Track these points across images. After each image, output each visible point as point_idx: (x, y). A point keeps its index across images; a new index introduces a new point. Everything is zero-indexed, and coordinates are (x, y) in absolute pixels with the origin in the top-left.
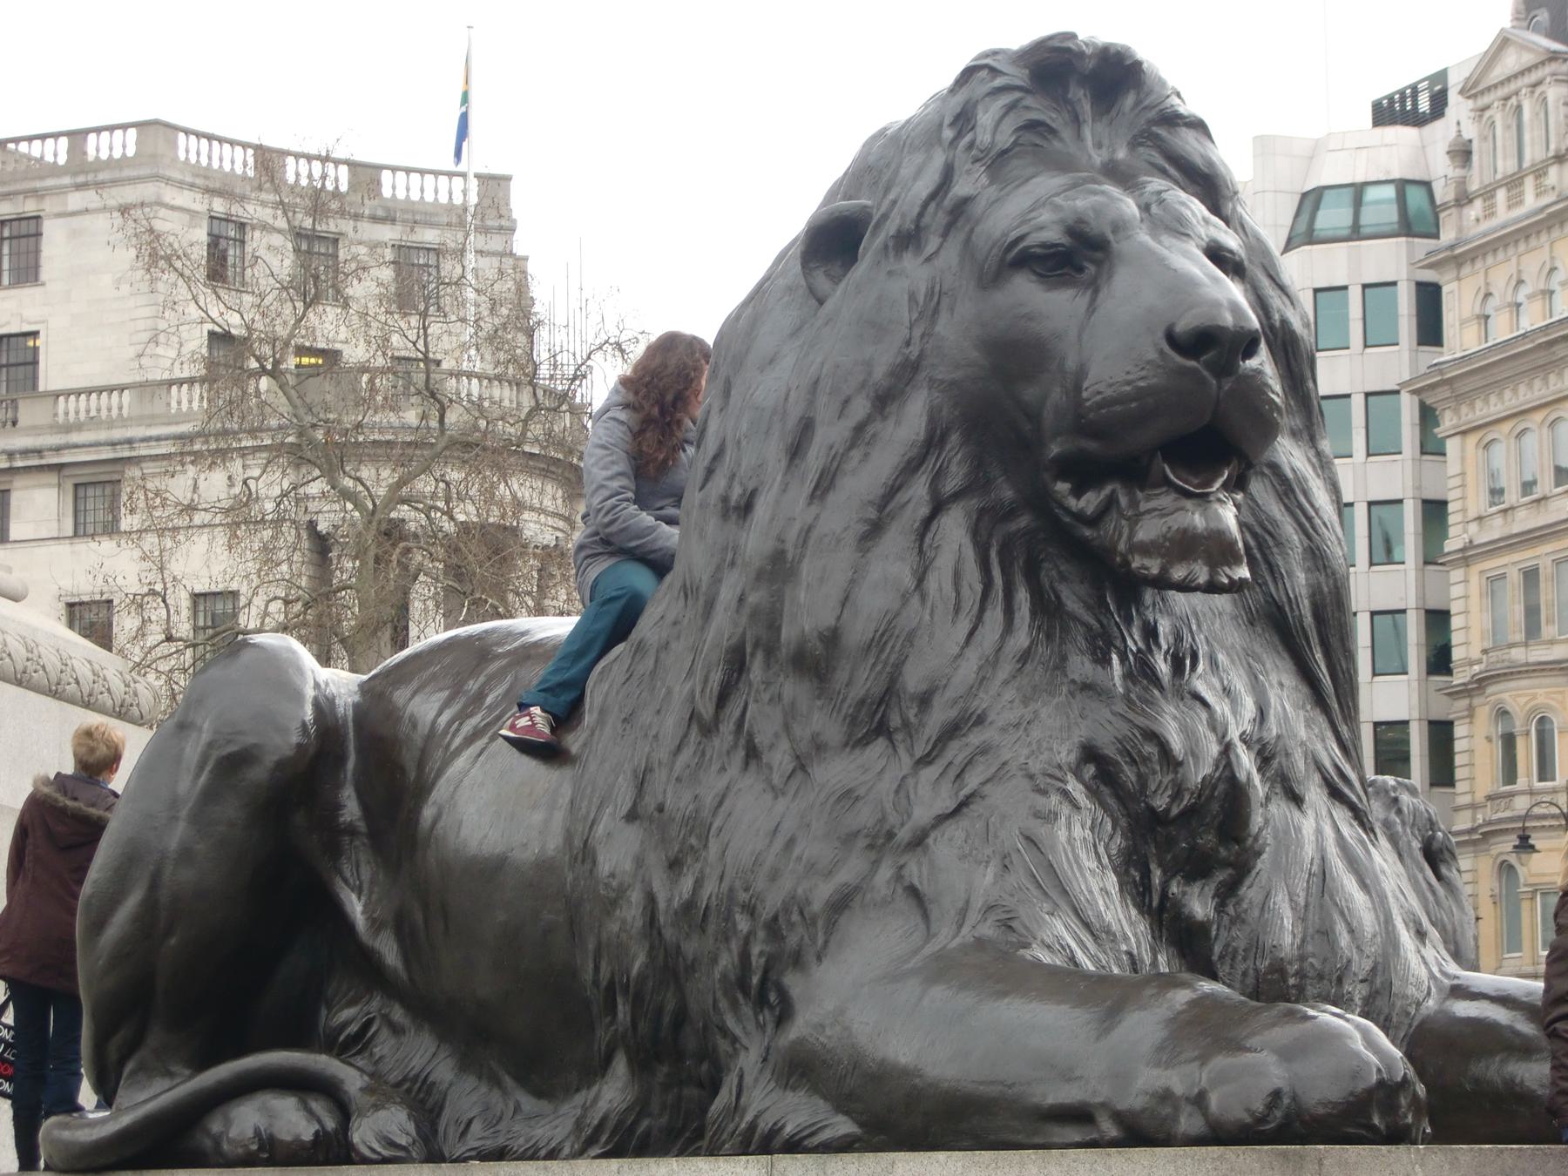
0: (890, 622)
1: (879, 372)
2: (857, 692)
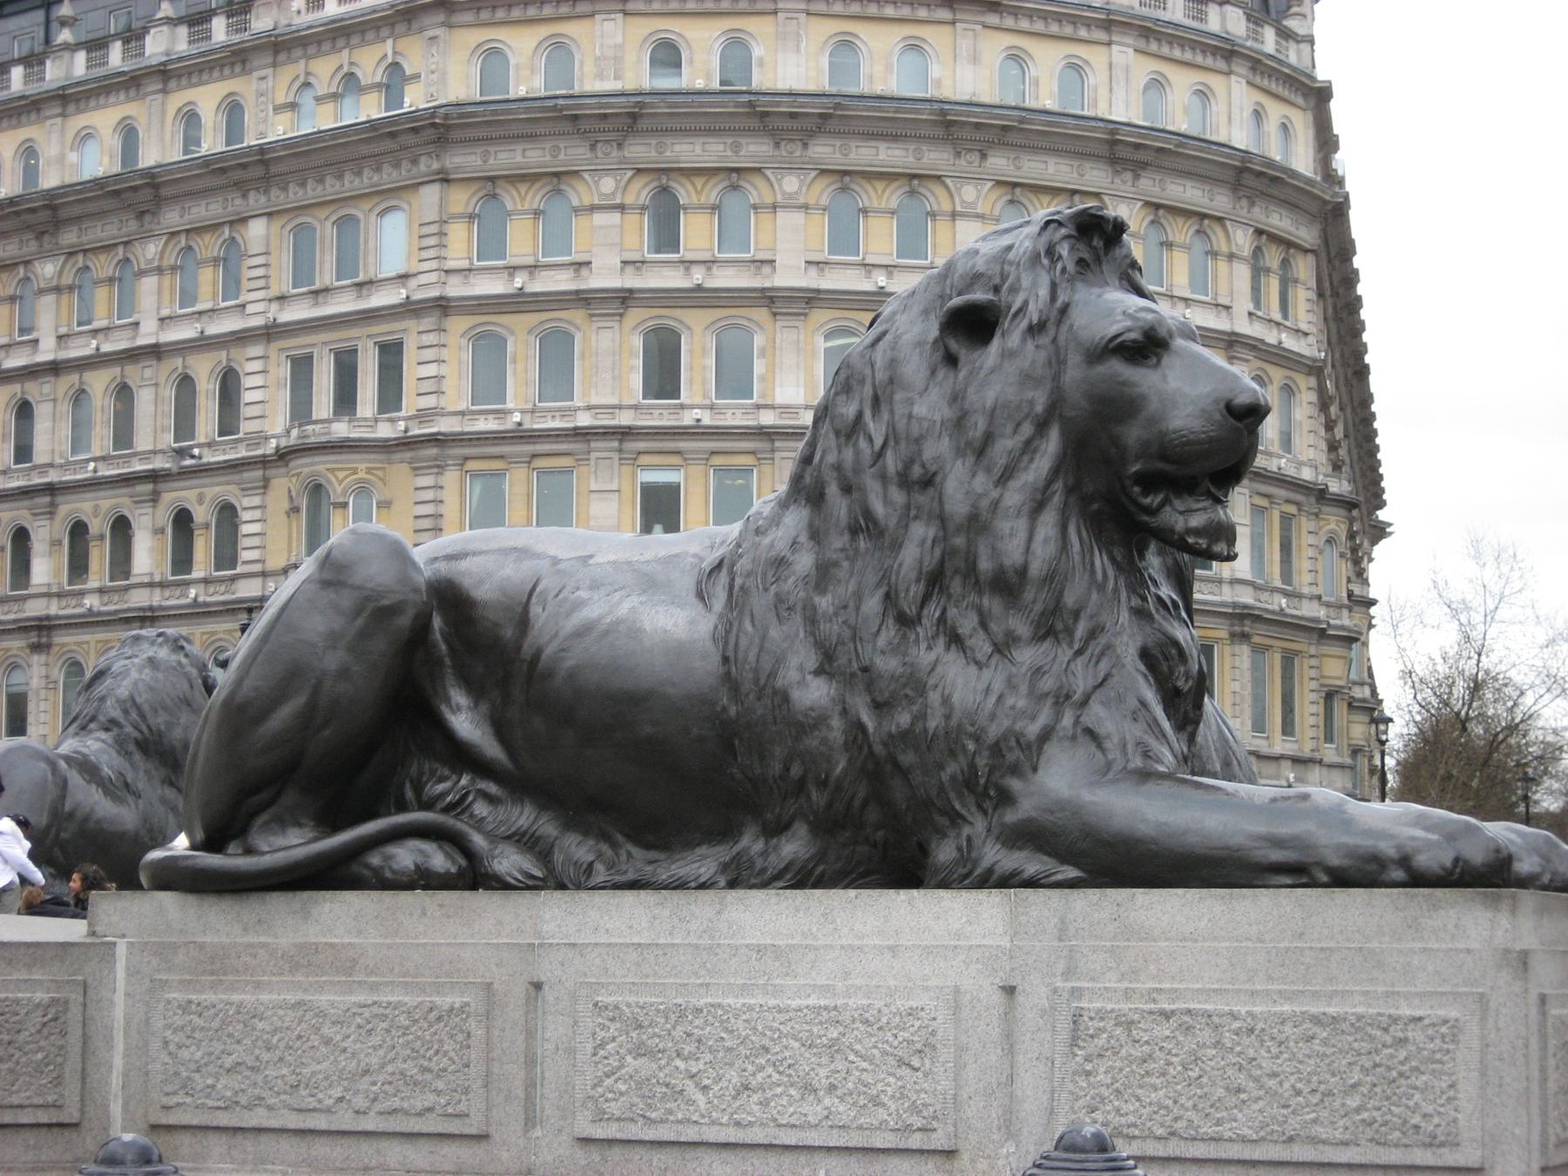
1: (1039, 408)
2: (1038, 607)
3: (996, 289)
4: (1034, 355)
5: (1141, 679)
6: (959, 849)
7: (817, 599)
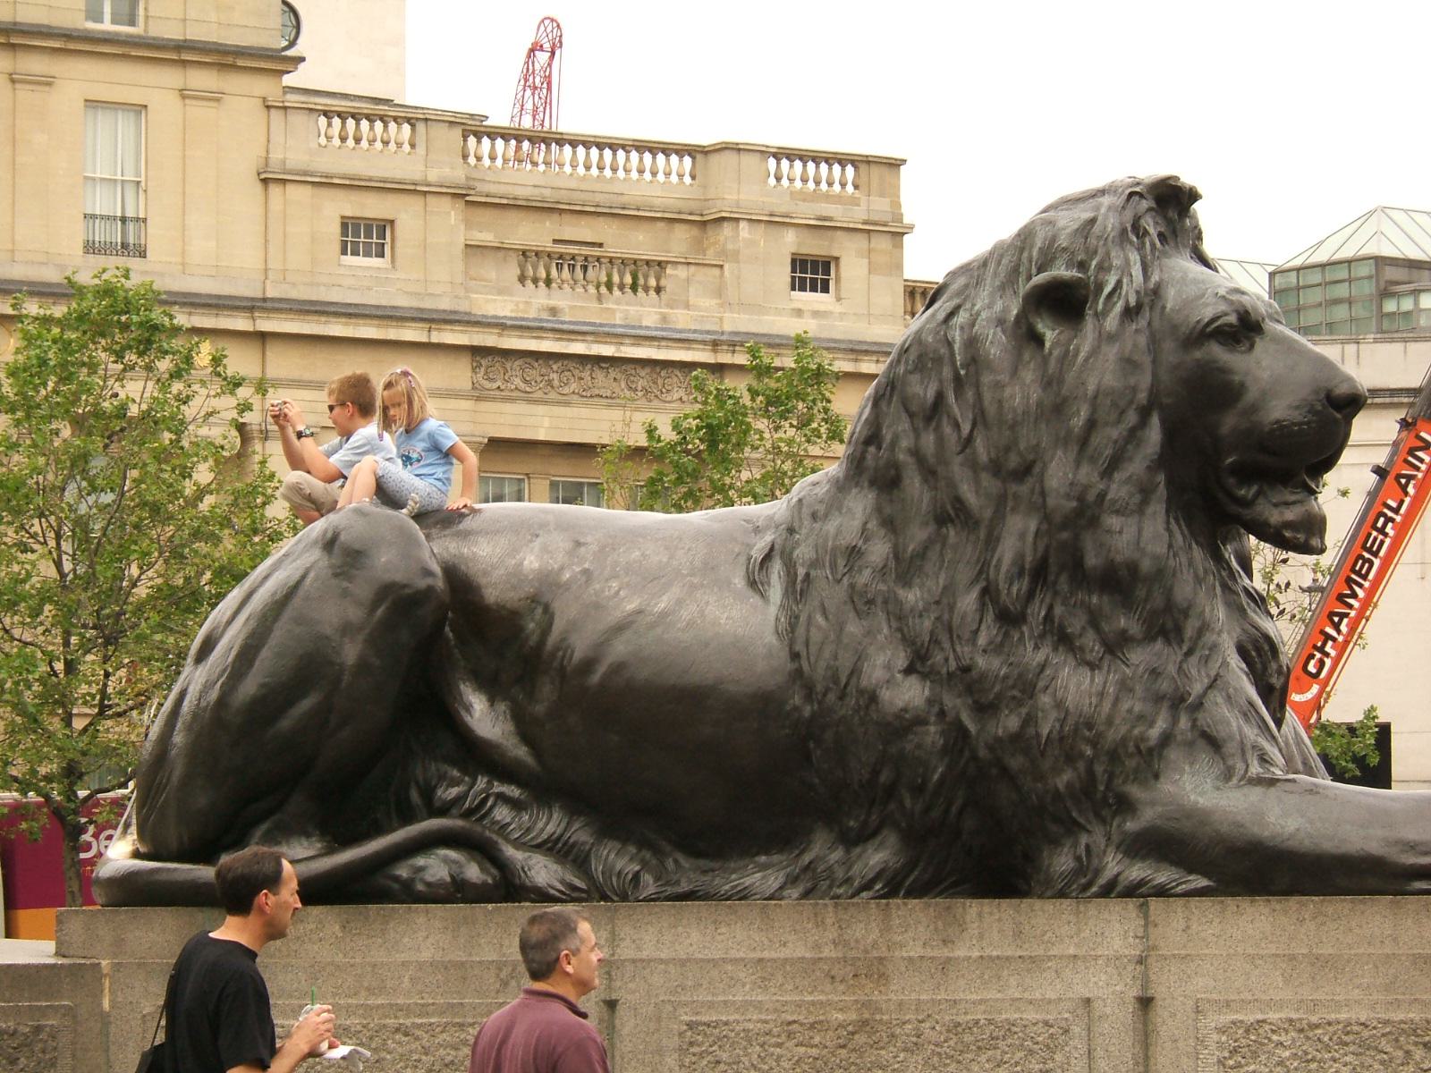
3: (1082, 266)
4: (1136, 337)
5: (1245, 677)
6: (1078, 859)
7: (901, 593)
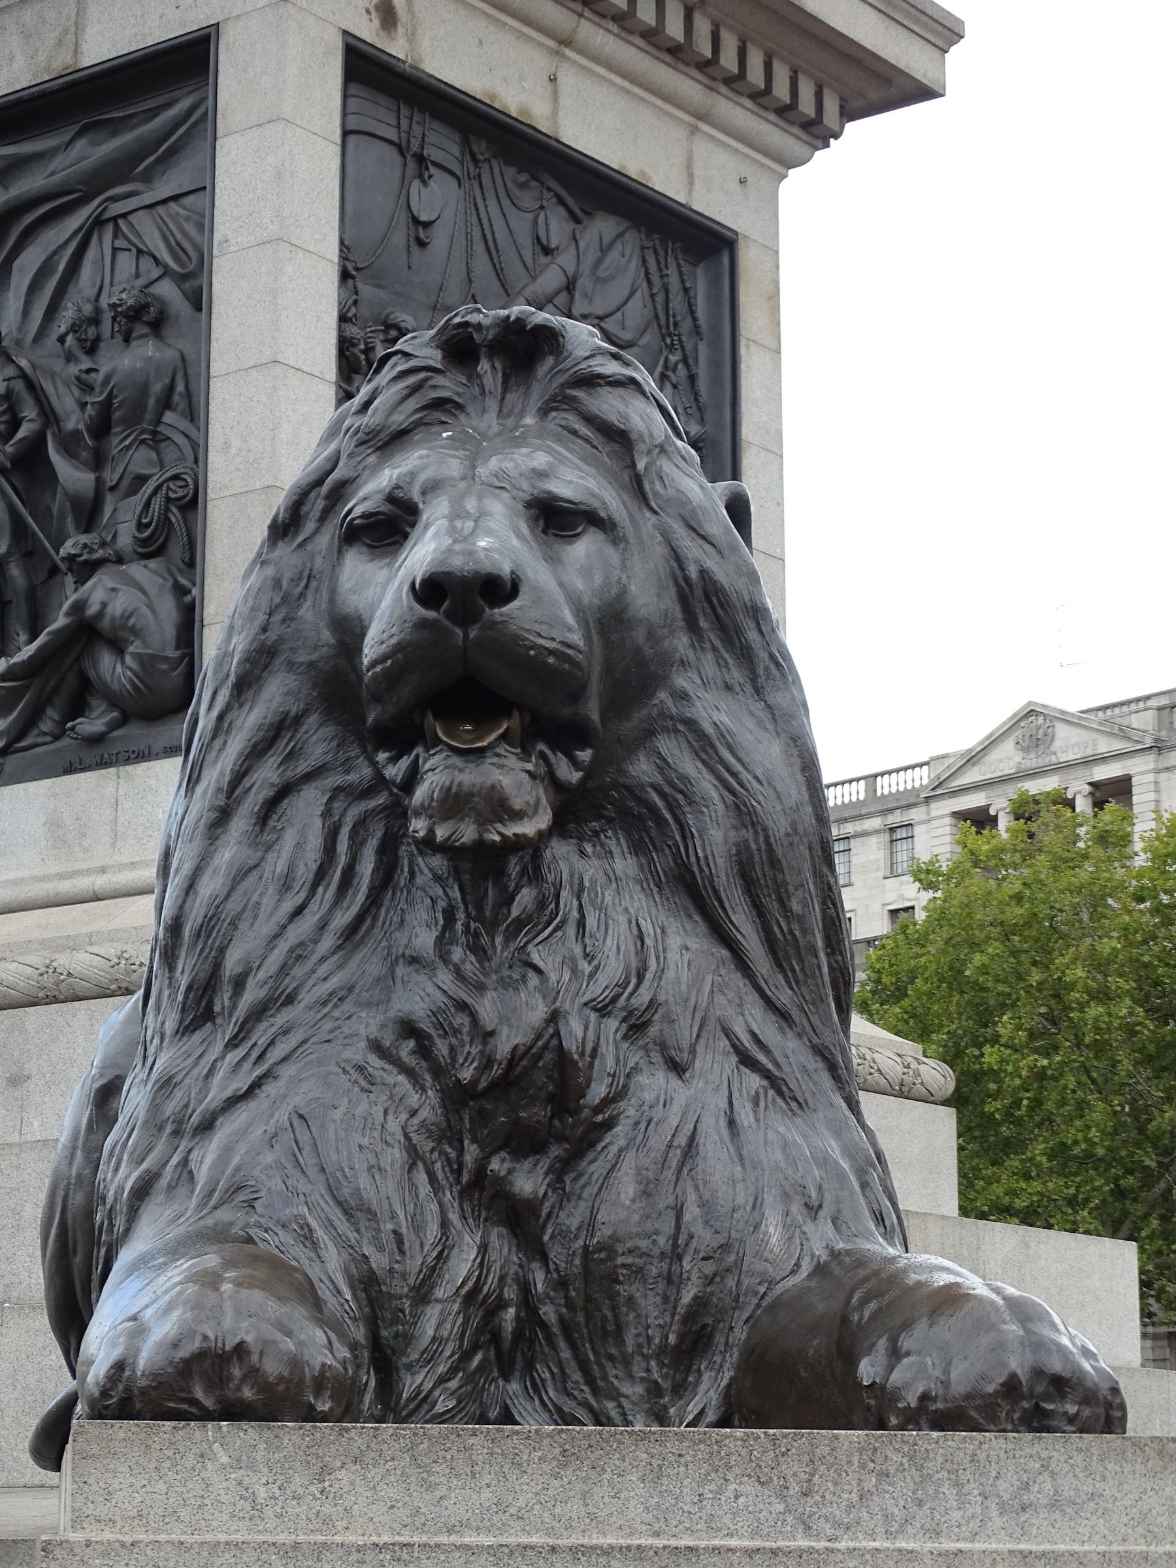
0: (218, 907)
